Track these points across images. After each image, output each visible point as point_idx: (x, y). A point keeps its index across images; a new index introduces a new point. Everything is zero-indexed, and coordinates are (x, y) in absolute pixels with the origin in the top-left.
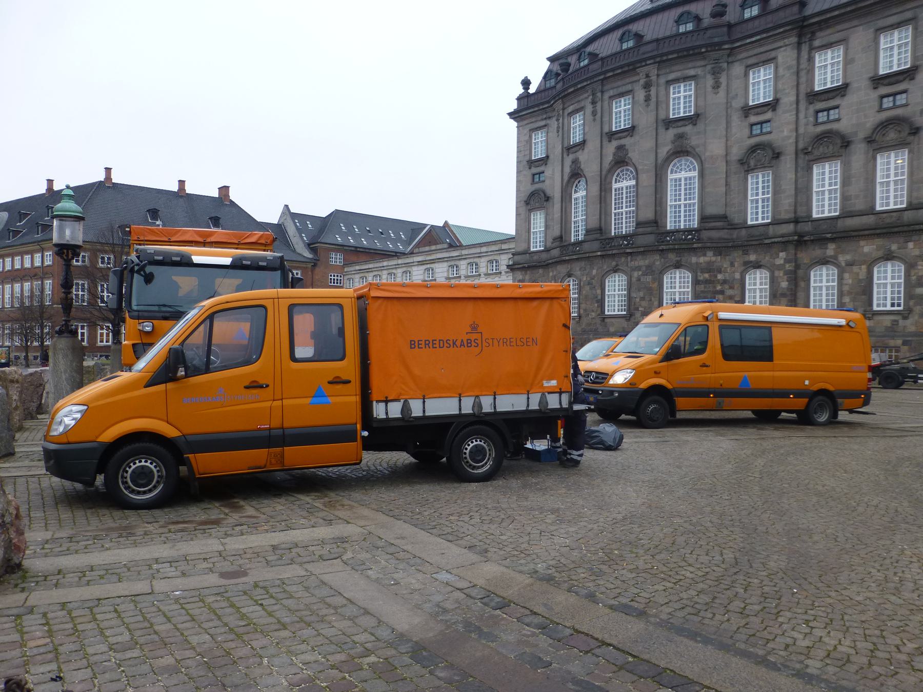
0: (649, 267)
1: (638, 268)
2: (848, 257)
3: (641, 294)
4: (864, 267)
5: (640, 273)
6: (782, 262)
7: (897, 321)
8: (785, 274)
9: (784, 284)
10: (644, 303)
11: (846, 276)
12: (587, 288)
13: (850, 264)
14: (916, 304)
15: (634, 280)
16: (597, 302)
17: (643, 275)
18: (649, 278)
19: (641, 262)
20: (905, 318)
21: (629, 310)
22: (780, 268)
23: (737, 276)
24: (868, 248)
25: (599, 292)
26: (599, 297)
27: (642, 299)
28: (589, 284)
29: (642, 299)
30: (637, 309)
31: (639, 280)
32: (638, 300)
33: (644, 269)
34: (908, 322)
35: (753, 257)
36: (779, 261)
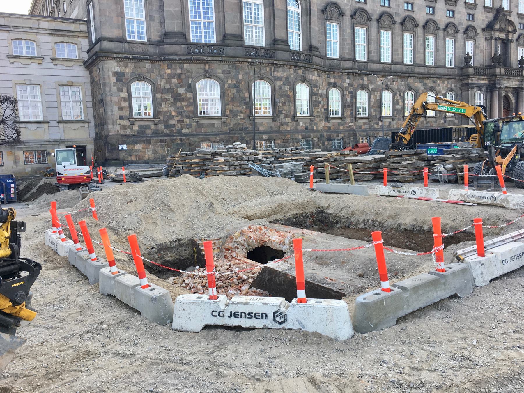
0: (287, 78)
1: (280, 78)
2: (373, 86)
3: (283, 100)
4: (379, 92)
5: (282, 82)
6: (348, 85)
7: (391, 122)
8: (349, 93)
9: (349, 100)
10: (286, 108)
11: (372, 97)
12: (234, 91)
13: (374, 90)
14: (397, 114)
15: (277, 88)
16: (245, 104)
17: (284, 84)
18: (287, 88)
19: (281, 73)
20: (393, 120)
21: (274, 111)
22: (347, 89)
23: (325, 92)
24: (379, 81)
25: (247, 95)
26: (248, 100)
27: (284, 104)
28: (235, 86)
29: (284, 104)
30: (281, 112)
31: (280, 88)
32: (281, 104)
33: (284, 79)
34: (395, 122)
35: (332, 81)
36: (346, 85)
